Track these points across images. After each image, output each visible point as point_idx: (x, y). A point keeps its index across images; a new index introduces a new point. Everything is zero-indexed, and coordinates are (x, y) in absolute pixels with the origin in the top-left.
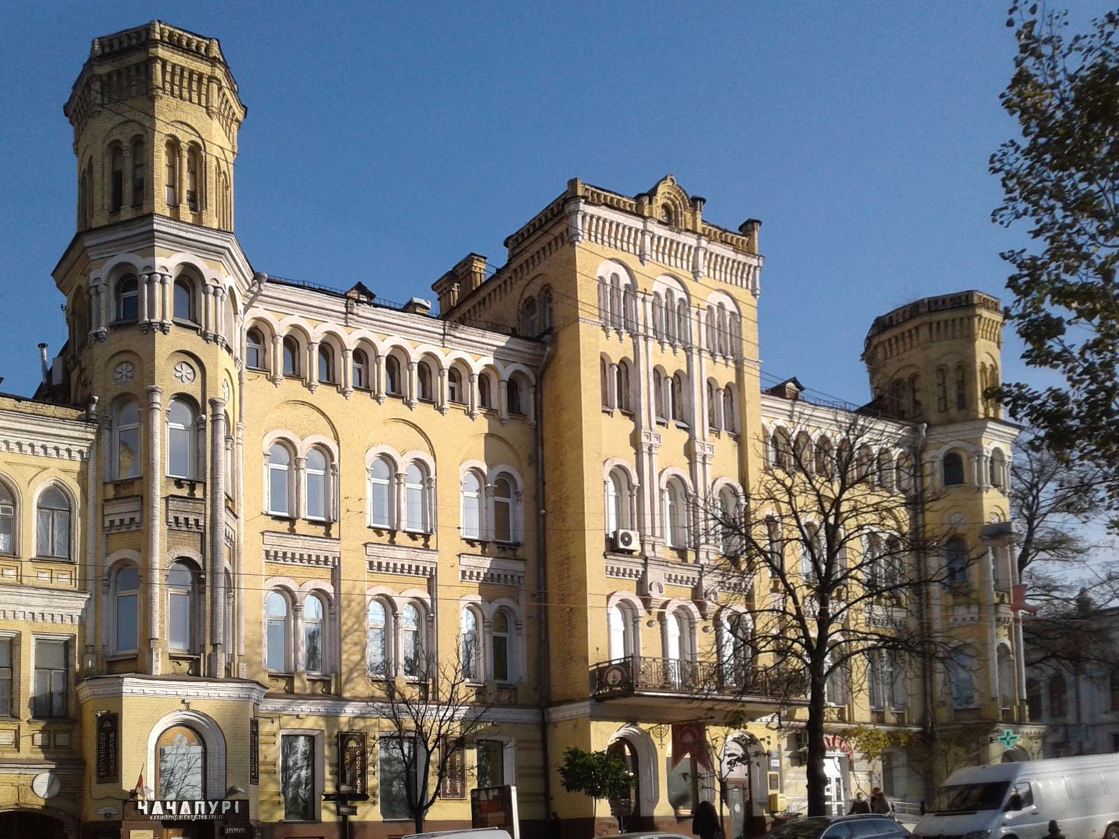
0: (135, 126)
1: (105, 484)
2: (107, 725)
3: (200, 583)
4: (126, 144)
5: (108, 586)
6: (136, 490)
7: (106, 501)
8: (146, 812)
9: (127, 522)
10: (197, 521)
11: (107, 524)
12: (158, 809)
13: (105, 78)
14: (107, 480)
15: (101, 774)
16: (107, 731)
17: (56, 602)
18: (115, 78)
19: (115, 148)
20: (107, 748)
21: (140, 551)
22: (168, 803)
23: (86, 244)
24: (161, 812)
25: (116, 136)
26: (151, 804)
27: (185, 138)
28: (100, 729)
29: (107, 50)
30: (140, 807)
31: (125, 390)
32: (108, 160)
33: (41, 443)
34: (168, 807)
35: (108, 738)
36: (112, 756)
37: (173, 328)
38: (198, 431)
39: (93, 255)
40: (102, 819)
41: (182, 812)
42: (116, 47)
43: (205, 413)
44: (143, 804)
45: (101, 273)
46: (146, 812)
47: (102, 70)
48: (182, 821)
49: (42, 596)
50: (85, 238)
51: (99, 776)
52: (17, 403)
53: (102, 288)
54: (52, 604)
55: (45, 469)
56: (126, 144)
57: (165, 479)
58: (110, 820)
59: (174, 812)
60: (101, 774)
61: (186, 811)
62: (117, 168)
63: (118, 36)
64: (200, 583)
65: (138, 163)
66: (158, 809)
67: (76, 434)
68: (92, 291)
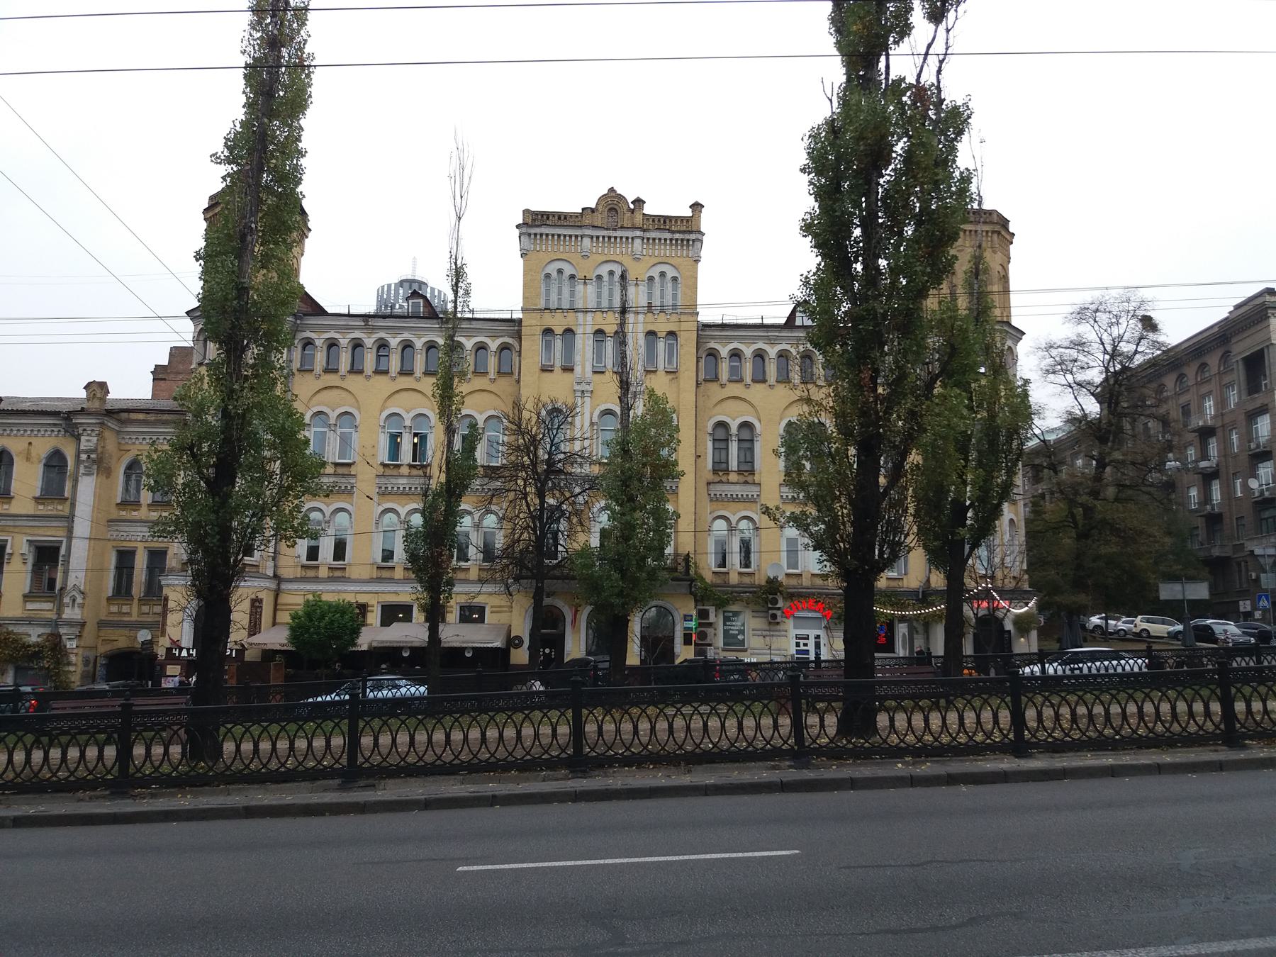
12: (184, 653)
26: (181, 649)
66: (184, 653)
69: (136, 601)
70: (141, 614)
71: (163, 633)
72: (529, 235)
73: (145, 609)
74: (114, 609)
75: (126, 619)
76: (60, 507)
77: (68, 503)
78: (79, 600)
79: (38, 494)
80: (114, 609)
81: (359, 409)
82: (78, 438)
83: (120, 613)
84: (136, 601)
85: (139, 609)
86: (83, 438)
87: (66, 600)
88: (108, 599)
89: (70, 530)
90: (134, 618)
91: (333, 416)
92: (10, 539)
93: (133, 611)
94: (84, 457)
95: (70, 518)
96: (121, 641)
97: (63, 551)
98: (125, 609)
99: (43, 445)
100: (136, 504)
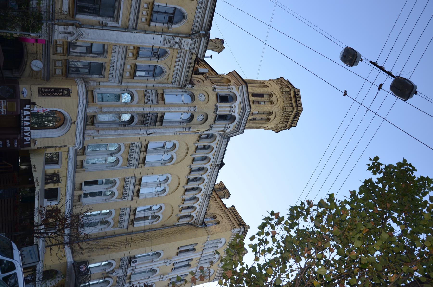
0: (276, 102)
1: (163, 90)
2: (66, 92)
3: (124, 125)
4: (271, 99)
5: (124, 90)
6: (160, 102)
7: (157, 90)
8: (24, 108)
9: (149, 98)
10: (148, 123)
11: (148, 91)
12: (26, 113)
13: (289, 93)
14: (164, 90)
15: (43, 89)
16: (62, 92)
17: (118, 72)
18: (289, 96)
19: (270, 95)
20: (55, 92)
21: (137, 103)
22: (29, 117)
23: (243, 86)
24: (24, 114)
25: (274, 96)
26: (29, 110)
27: (272, 117)
28: (63, 89)
29: (297, 93)
30: (27, 106)
31: (196, 97)
32: (267, 93)
33: (179, 68)
35: (60, 92)
36: (51, 95)
37: (215, 114)
39: (240, 87)
40: (21, 90)
41: (24, 122)
42: (297, 96)
43: (186, 125)
45: (235, 90)
46: (24, 108)
47: (292, 93)
49: (121, 67)
50: (245, 86)
51: (42, 89)
53: (230, 90)
54: (117, 70)
55: (170, 69)
56: (271, 99)
58: (21, 94)
59: (24, 119)
60: (43, 89)
61: (25, 124)
62: (265, 96)
63: (300, 97)
64: (124, 125)
65: (266, 102)
66: (26, 113)
67: (181, 81)
68: (229, 87)
69: (65, 58)
70: (55, 61)
72: (239, 232)
73: (59, 64)
75: (51, 51)
76: (143, 20)
77: (146, 26)
81: (174, 164)
82: (190, 35)
84: (65, 58)
86: (190, 40)
87: (70, 29)
90: (52, 57)
91: (173, 153)
94: (177, 39)
95: (135, 29)
97: (110, 23)
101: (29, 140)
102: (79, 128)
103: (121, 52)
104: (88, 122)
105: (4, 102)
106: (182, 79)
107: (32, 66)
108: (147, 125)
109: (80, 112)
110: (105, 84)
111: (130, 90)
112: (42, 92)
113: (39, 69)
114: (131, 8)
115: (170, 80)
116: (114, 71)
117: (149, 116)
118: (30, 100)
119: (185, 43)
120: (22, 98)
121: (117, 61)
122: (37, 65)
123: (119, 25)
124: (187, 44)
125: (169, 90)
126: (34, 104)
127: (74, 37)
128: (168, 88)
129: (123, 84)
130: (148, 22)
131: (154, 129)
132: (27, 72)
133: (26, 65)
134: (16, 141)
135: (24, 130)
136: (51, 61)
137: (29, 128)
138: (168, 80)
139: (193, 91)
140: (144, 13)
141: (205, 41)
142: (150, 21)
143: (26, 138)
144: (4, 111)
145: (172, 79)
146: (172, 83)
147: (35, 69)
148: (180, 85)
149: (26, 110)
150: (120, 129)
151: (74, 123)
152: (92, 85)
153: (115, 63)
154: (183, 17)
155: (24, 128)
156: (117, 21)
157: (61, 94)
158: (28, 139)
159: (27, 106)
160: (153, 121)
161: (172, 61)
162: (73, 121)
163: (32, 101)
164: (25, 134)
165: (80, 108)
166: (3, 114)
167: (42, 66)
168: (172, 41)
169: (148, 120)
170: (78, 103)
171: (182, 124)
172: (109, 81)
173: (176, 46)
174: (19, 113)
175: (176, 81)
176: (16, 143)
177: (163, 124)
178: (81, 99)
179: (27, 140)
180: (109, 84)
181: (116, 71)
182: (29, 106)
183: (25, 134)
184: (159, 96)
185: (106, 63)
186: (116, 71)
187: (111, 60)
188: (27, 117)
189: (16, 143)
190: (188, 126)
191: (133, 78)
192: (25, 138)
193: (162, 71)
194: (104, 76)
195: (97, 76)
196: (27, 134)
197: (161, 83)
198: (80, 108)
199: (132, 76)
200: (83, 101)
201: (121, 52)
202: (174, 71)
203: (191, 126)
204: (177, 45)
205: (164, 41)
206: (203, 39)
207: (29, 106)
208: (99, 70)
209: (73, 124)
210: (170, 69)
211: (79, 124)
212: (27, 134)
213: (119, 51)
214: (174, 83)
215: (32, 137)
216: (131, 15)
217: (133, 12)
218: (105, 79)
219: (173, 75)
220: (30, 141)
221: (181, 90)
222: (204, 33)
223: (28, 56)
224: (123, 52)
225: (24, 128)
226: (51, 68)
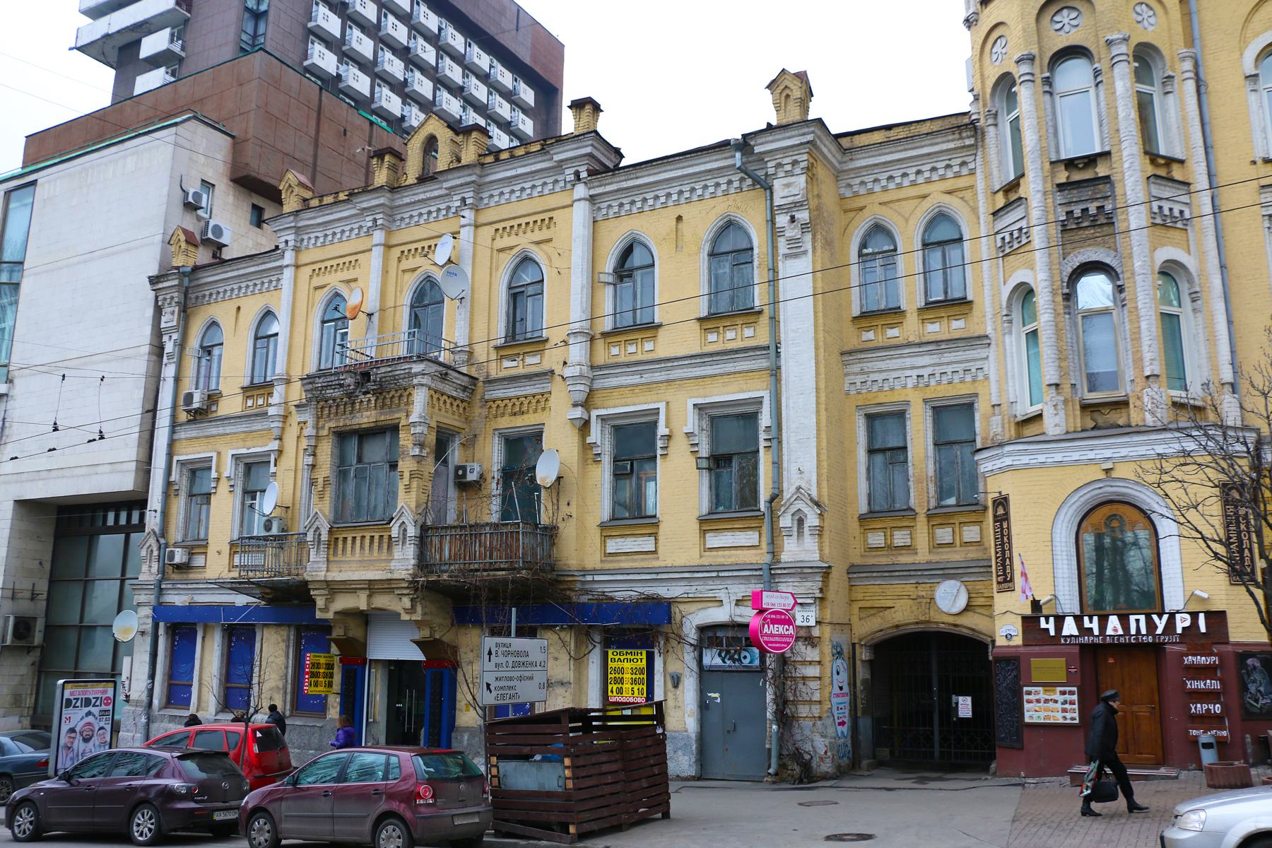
2: (1001, 511)
5: (1010, 322)
8: (1052, 633)
12: (1070, 628)
14: (997, 187)
17: (948, 357)
22: (1086, 619)
24: (1076, 633)
26: (1060, 620)
30: (1043, 625)
34: (1087, 624)
38: (1097, 85)
41: (1109, 632)
44: (1047, 622)
46: (1052, 633)
48: (1112, 645)
51: (999, 583)
52: (888, 133)
55: (925, 197)
57: (1047, 166)
58: (1012, 643)
59: (1096, 632)
61: (1115, 630)
66: (1070, 628)
67: (951, 145)
69: (921, 522)
70: (937, 546)
71: (1006, 581)
73: (944, 534)
74: (876, 539)
75: (905, 559)
76: (748, 332)
78: (812, 520)
79: (704, 313)
80: (876, 539)
82: (766, 186)
83: (890, 548)
85: (932, 536)
86: (777, 184)
87: (786, 521)
88: (862, 519)
89: (775, 372)
90: (923, 555)
92: (662, 406)
93: (920, 542)
94: (782, 220)
96: (901, 610)
97: (765, 420)
98: (900, 538)
99: (702, 219)
100: (894, 314)
101: (1188, 617)
102: (1124, 452)
103: (883, 365)
104: (1121, 422)
105: (1029, 693)
106: (944, 146)
107: (955, 610)
108: (1109, 207)
109: (1058, 457)
110: (994, 387)
111: (1004, 304)
112: (1005, 581)
113: (963, 589)
114: (722, 375)
115: (962, 183)
116: (949, 369)
117: (1070, 213)
118: (1025, 619)
119: (786, 193)
120: (1018, 641)
121: (913, 368)
122: (950, 599)
123: (766, 395)
124: (788, 185)
125: (995, 172)
126: (1036, 605)
127: (806, 510)
128: (988, 176)
129: (989, 331)
130: (752, 319)
131: (1122, 180)
132: (974, 622)
133: (956, 625)
134: (1189, 660)
135: (1144, 631)
136: (934, 558)
137: (1132, 618)
138: (966, 188)
139: (989, 90)
140: (733, 337)
141: (760, 141)
142: (751, 314)
143: (1182, 622)
144: (1063, 693)
145: (958, 175)
146: (972, 173)
147: (962, 602)
148: (968, 142)
149: (1103, 626)
150: (1135, 299)
151: (1107, 471)
152: (1000, 429)
153: (920, 372)
154: (729, 226)
155: (1133, 631)
156: (759, 401)
157: (1005, 525)
158: (1183, 620)
159: (1043, 625)
160: (1087, 193)
161: (899, 200)
162: (1102, 476)
163: (1028, 611)
164: (1159, 631)
165: (1042, 458)
166: (1075, 697)
167: (952, 582)
168: (789, 234)
169: (1085, 210)
170: (1027, 467)
171: (1099, 79)
172: (987, 378)
173: (803, 216)
174: (1076, 650)
175: (959, 161)
176: (1202, 660)
177: (1107, 149)
178: (1008, 461)
179: (1187, 624)
180: (993, 377)
181: (948, 364)
182: (1043, 620)
183: (1159, 631)
184: (1013, 197)
185: (925, 401)
186: (948, 364)
187: (916, 387)
188: (1087, 624)
189: (1202, 660)
190: (1103, 52)
191: (971, 302)
192: (1179, 631)
193: (940, 217)
194: (971, 395)
195: (977, 416)
196: (1161, 624)
197: (975, 210)
198: (1042, 458)
199: (964, 309)
200: (1010, 454)
201: (883, 365)
202: (928, 181)
203: (1102, 42)
204: (798, 215)
205: (796, 256)
206: (757, 149)
207: (1043, 620)
208: (953, 416)
209: (1114, 474)
210: (925, 197)
211: (1108, 453)
212: (1161, 624)
213: (881, 371)
214: (971, 166)
215: (1180, 607)
216: (738, 369)
217: (730, 367)
218: (980, 389)
219: (943, 178)
220: (1194, 615)
221: (991, 131)
222: (738, 155)
223: (928, 622)
224: (882, 359)
225: (1133, 631)
226: (957, 557)
